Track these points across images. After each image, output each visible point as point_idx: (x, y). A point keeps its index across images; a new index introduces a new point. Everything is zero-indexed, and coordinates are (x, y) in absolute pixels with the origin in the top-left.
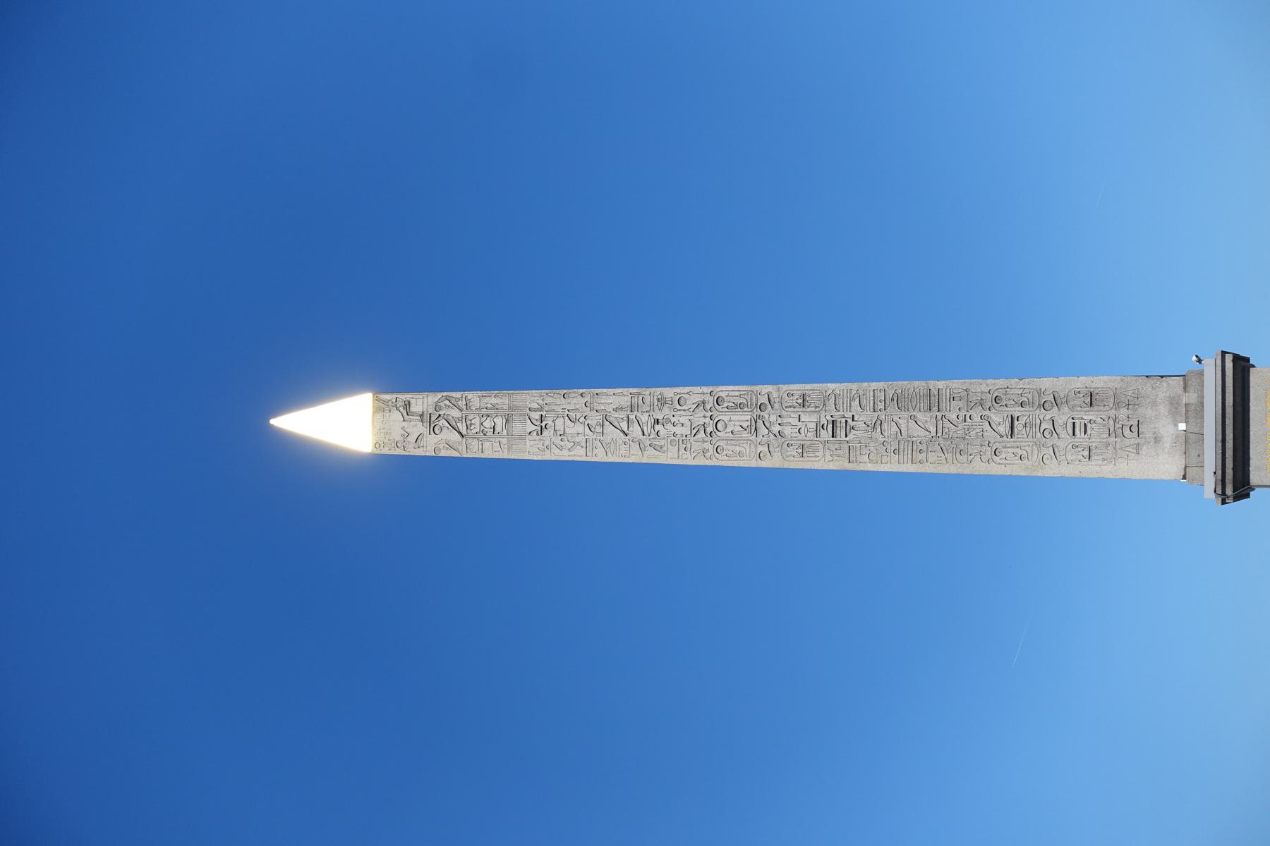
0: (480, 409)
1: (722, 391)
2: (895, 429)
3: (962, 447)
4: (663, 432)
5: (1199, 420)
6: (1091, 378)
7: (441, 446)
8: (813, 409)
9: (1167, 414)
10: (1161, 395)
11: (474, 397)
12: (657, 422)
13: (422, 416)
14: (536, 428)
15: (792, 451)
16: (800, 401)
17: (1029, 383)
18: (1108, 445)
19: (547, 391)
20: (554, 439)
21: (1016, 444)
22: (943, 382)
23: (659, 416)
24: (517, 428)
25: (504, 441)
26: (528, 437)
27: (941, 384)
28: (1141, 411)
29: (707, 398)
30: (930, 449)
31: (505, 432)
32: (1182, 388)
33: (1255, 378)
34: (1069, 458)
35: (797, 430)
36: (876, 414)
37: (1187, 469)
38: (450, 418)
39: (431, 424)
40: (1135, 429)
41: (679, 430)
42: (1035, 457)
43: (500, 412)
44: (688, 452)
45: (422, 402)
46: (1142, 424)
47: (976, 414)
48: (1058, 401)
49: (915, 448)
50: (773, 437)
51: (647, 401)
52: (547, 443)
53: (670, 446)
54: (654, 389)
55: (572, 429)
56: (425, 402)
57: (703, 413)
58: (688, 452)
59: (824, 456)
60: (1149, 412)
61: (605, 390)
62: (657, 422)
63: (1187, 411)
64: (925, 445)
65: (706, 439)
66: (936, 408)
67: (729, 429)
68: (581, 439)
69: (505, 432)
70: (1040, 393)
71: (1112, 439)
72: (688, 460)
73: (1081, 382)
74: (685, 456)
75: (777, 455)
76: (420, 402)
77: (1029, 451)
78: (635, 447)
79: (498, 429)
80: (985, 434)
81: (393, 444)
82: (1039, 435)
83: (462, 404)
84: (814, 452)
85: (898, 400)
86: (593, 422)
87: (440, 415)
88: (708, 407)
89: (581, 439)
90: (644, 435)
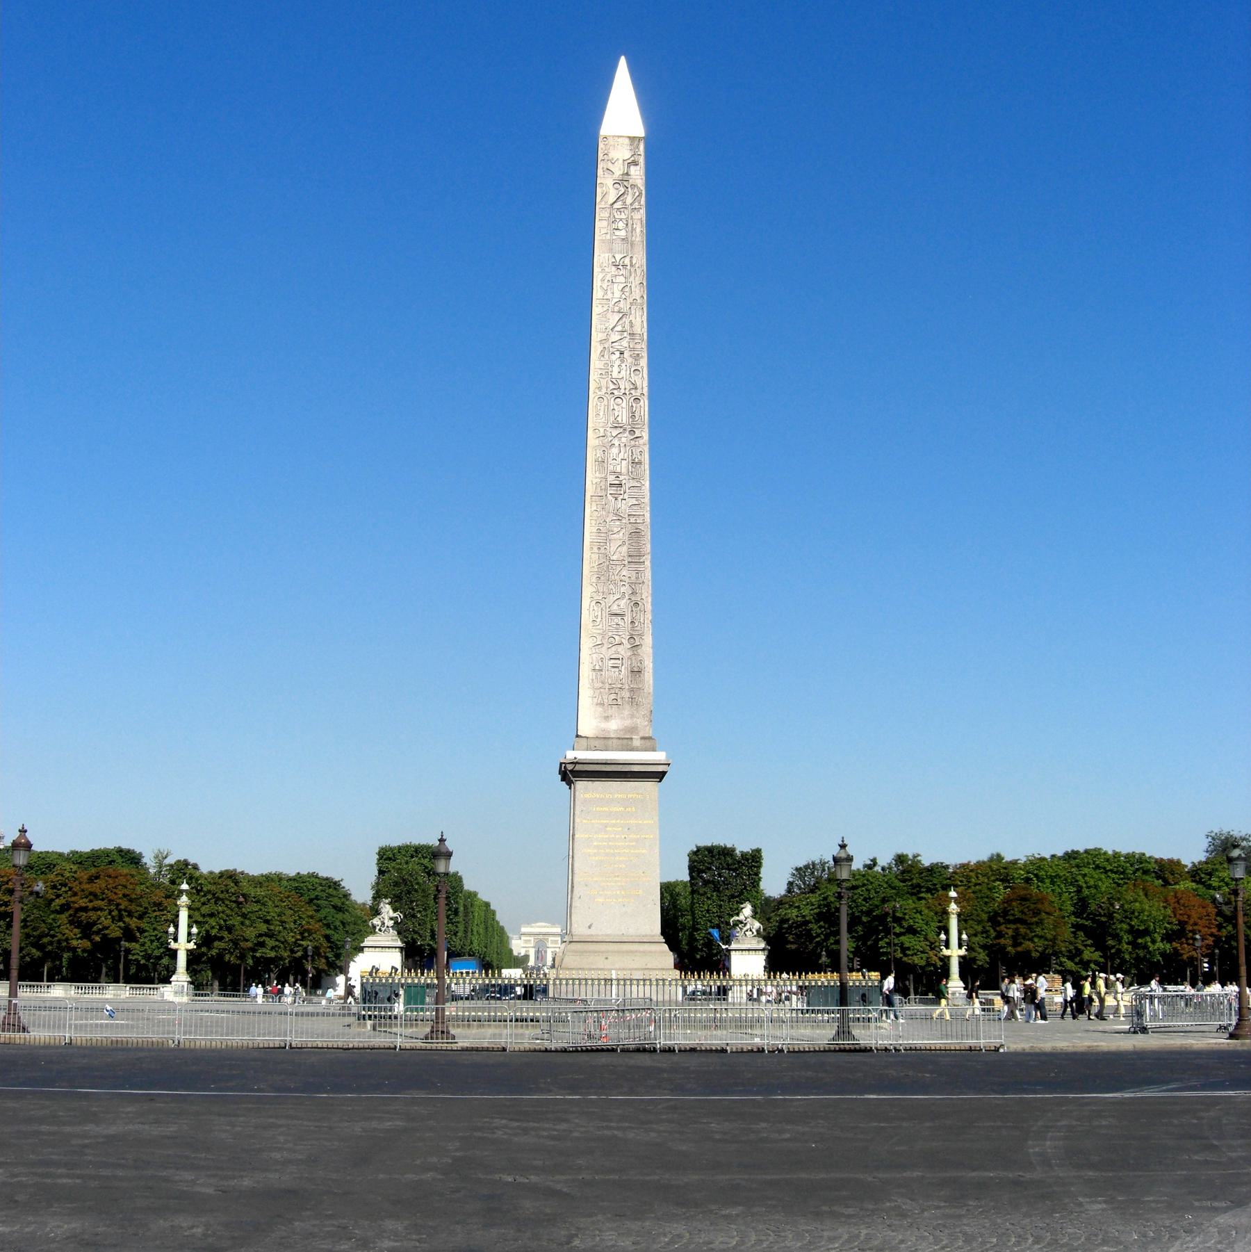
1: (645, 403)
2: (616, 530)
3: (602, 578)
4: (614, 357)
5: (620, 747)
6: (651, 671)
7: (604, 188)
8: (630, 470)
9: (625, 725)
10: (638, 721)
11: (641, 215)
12: (622, 353)
13: (627, 174)
16: (637, 460)
17: (648, 627)
18: (603, 683)
19: (645, 270)
20: (609, 275)
21: (604, 617)
22: (649, 565)
23: (626, 355)
24: (618, 246)
25: (608, 237)
26: (611, 256)
27: (648, 563)
28: (627, 707)
29: (639, 391)
30: (600, 555)
31: (614, 237)
32: (643, 735)
33: (649, 786)
34: (595, 655)
35: (615, 457)
36: (626, 516)
37: (585, 739)
38: (625, 196)
39: (624, 180)
40: (615, 702)
41: (616, 369)
42: (595, 631)
43: (630, 234)
44: (599, 376)
45: (638, 175)
46: (618, 707)
47: (626, 589)
48: (634, 649)
49: (602, 546)
50: (610, 439)
51: (638, 346)
54: (646, 352)
57: (628, 388)
58: (599, 376)
59: (596, 478)
60: (626, 713)
61: (645, 314)
62: (622, 353)
63: (627, 738)
66: (630, 560)
67: (616, 407)
68: (609, 296)
69: (614, 237)
70: (641, 635)
71: (607, 686)
72: (594, 376)
73: (649, 664)
74: (596, 373)
75: (597, 442)
76: (638, 173)
77: (598, 627)
78: (603, 336)
79: (617, 233)
80: (612, 595)
81: (606, 152)
82: (610, 634)
83: (636, 205)
84: (599, 470)
85: (636, 534)
86: (622, 304)
87: (627, 188)
88: (633, 392)
89: (609, 296)
90: (612, 343)
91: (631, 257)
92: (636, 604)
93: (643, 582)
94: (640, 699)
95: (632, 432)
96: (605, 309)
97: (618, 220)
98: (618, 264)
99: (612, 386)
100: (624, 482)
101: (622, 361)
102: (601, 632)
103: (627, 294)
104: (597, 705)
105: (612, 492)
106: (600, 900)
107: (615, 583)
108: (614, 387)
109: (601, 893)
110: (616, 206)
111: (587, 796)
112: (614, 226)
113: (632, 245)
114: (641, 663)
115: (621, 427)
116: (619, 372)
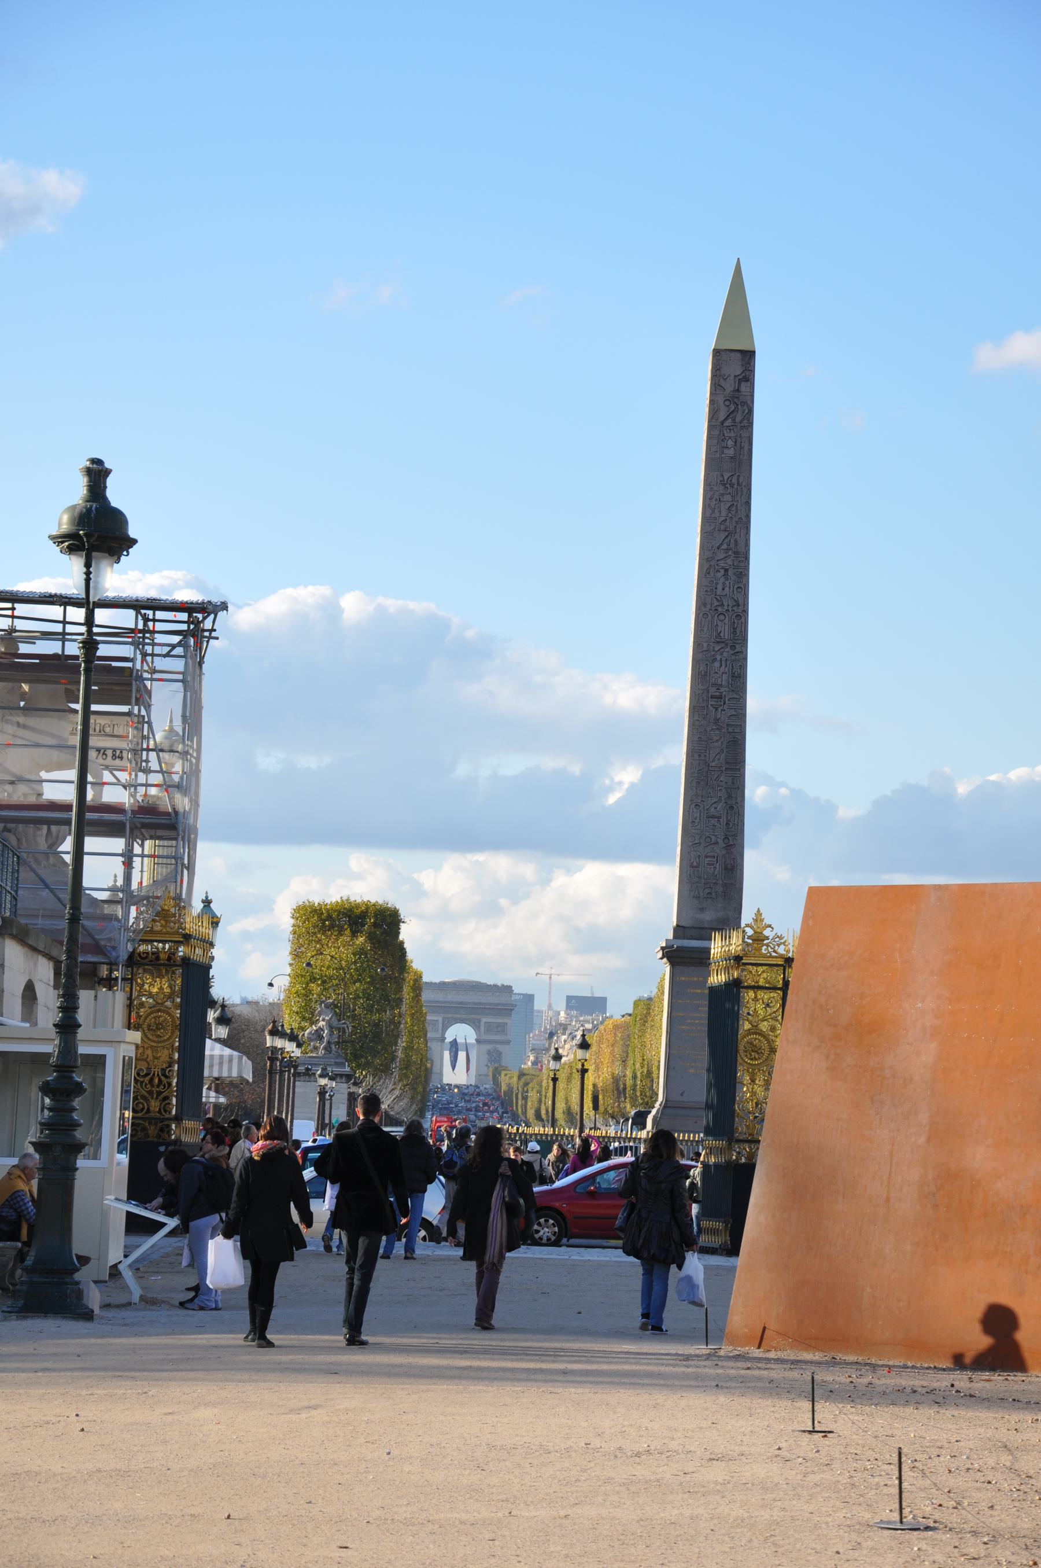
0: (740, 437)
2: (715, 738)
3: (702, 783)
4: (719, 575)
7: (715, 405)
12: (726, 571)
13: (738, 390)
14: (726, 479)
15: (703, 668)
18: (700, 878)
20: (718, 493)
21: (702, 818)
23: (730, 573)
26: (719, 475)
29: (741, 607)
31: (723, 455)
36: (725, 726)
38: (736, 413)
41: (720, 587)
42: (693, 831)
47: (723, 794)
50: (713, 653)
52: (715, 488)
53: (709, 580)
55: (724, 507)
56: (747, 394)
59: (699, 689)
62: (726, 571)
64: (704, 758)
65: (713, 606)
66: (727, 766)
68: (717, 514)
70: (735, 835)
74: (702, 590)
76: (748, 389)
79: (726, 451)
82: (707, 834)
86: (728, 523)
87: (737, 405)
88: (734, 608)
90: (718, 561)
91: (739, 476)
92: (732, 808)
93: (738, 788)
94: (732, 893)
95: (733, 647)
96: (712, 528)
97: (727, 438)
98: (725, 482)
99: (716, 603)
100: (724, 693)
101: (727, 579)
102: (699, 832)
103: (733, 513)
104: (693, 897)
105: (713, 703)
106: (692, 1071)
107: (713, 788)
108: (718, 604)
109: (693, 1064)
110: (729, 422)
111: (683, 979)
112: (724, 444)
113: (739, 463)
114: (734, 861)
115: (723, 642)
116: (723, 589)
